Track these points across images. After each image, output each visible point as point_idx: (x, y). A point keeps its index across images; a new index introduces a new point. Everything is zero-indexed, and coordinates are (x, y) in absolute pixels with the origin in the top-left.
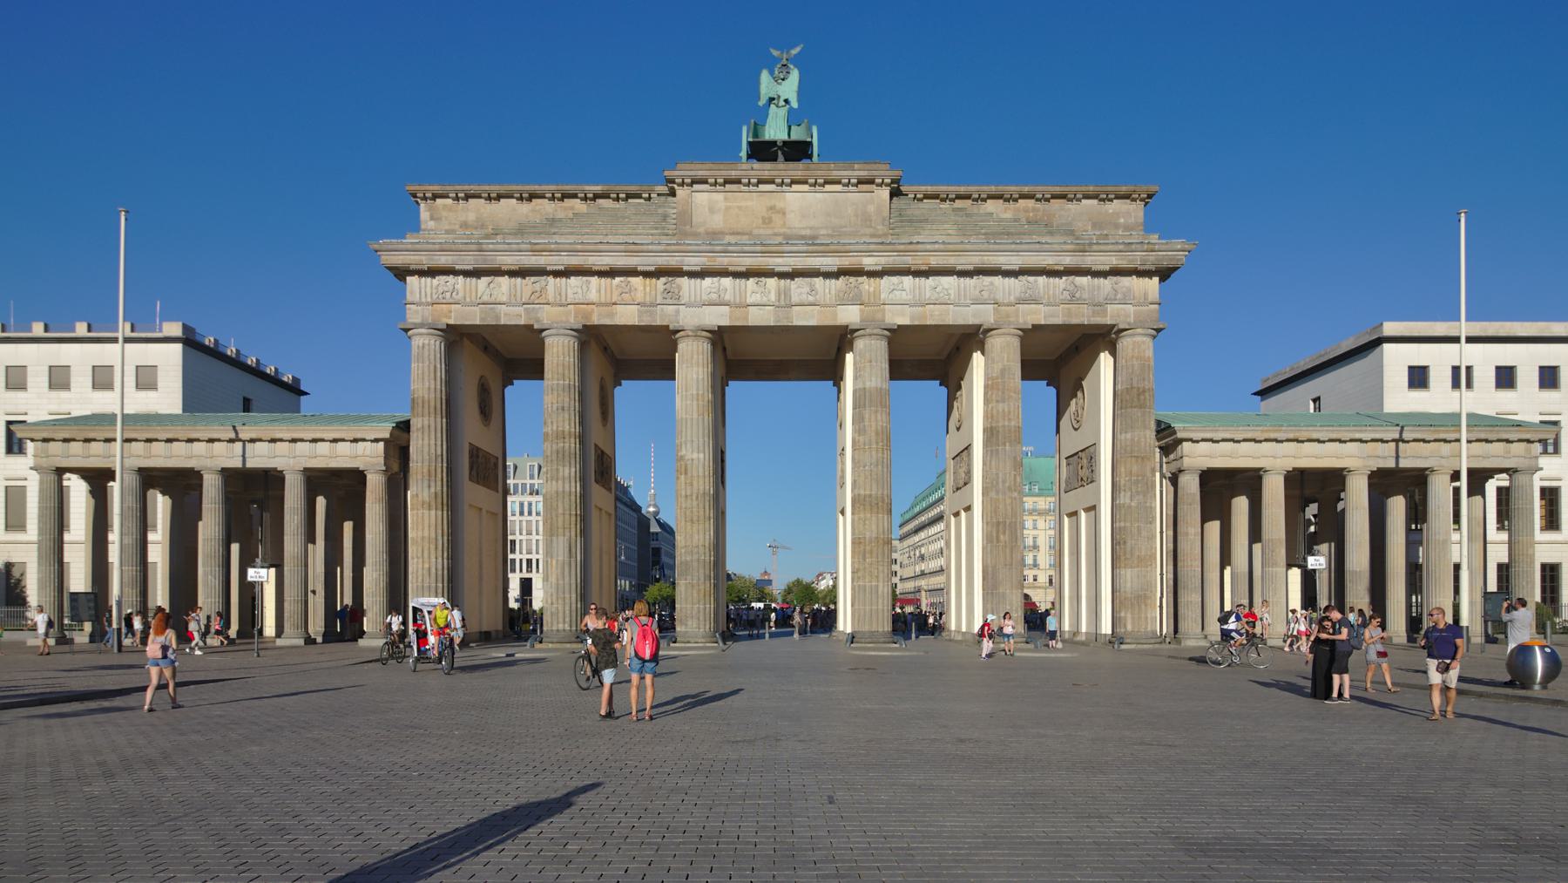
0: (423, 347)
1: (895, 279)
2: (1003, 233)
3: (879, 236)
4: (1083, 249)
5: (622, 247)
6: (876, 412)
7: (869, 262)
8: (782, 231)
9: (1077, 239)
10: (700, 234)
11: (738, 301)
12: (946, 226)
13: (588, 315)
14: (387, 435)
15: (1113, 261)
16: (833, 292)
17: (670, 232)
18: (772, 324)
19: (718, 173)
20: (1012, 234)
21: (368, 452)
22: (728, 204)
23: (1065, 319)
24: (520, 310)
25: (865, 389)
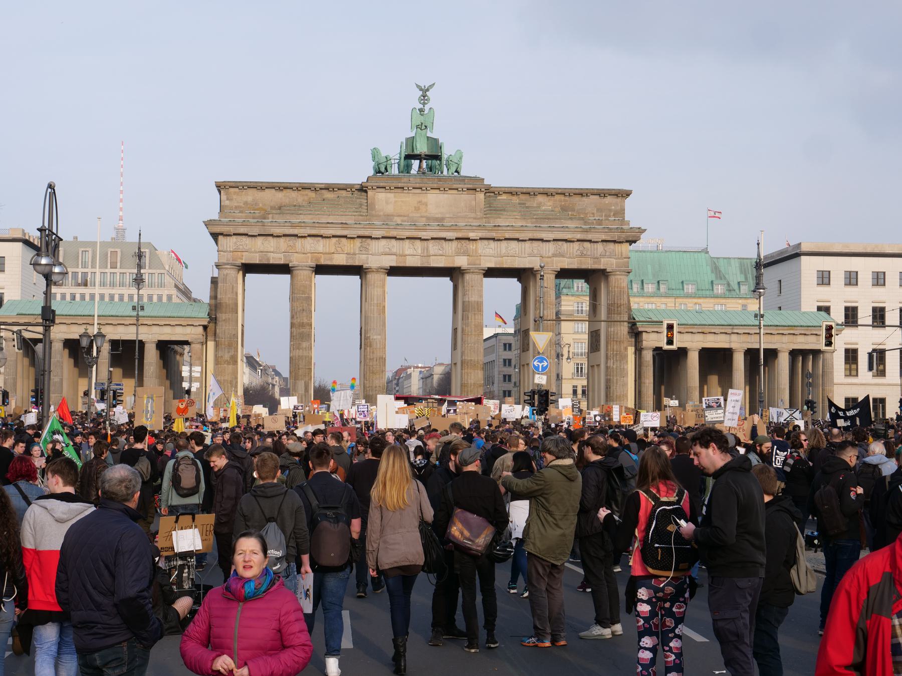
0: (227, 275)
1: (486, 242)
2: (546, 219)
3: (478, 219)
4: (586, 231)
5: (341, 226)
6: (475, 314)
7: (472, 235)
8: (425, 214)
9: (586, 223)
10: (380, 216)
11: (401, 253)
12: (515, 213)
13: (318, 259)
14: (206, 323)
15: (604, 237)
16: (453, 249)
17: (364, 214)
18: (419, 265)
19: (391, 184)
20: (550, 219)
21: (192, 332)
22: (397, 199)
23: (579, 265)
24: (281, 256)
25: (469, 301)
